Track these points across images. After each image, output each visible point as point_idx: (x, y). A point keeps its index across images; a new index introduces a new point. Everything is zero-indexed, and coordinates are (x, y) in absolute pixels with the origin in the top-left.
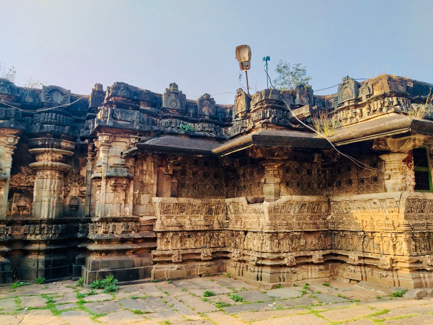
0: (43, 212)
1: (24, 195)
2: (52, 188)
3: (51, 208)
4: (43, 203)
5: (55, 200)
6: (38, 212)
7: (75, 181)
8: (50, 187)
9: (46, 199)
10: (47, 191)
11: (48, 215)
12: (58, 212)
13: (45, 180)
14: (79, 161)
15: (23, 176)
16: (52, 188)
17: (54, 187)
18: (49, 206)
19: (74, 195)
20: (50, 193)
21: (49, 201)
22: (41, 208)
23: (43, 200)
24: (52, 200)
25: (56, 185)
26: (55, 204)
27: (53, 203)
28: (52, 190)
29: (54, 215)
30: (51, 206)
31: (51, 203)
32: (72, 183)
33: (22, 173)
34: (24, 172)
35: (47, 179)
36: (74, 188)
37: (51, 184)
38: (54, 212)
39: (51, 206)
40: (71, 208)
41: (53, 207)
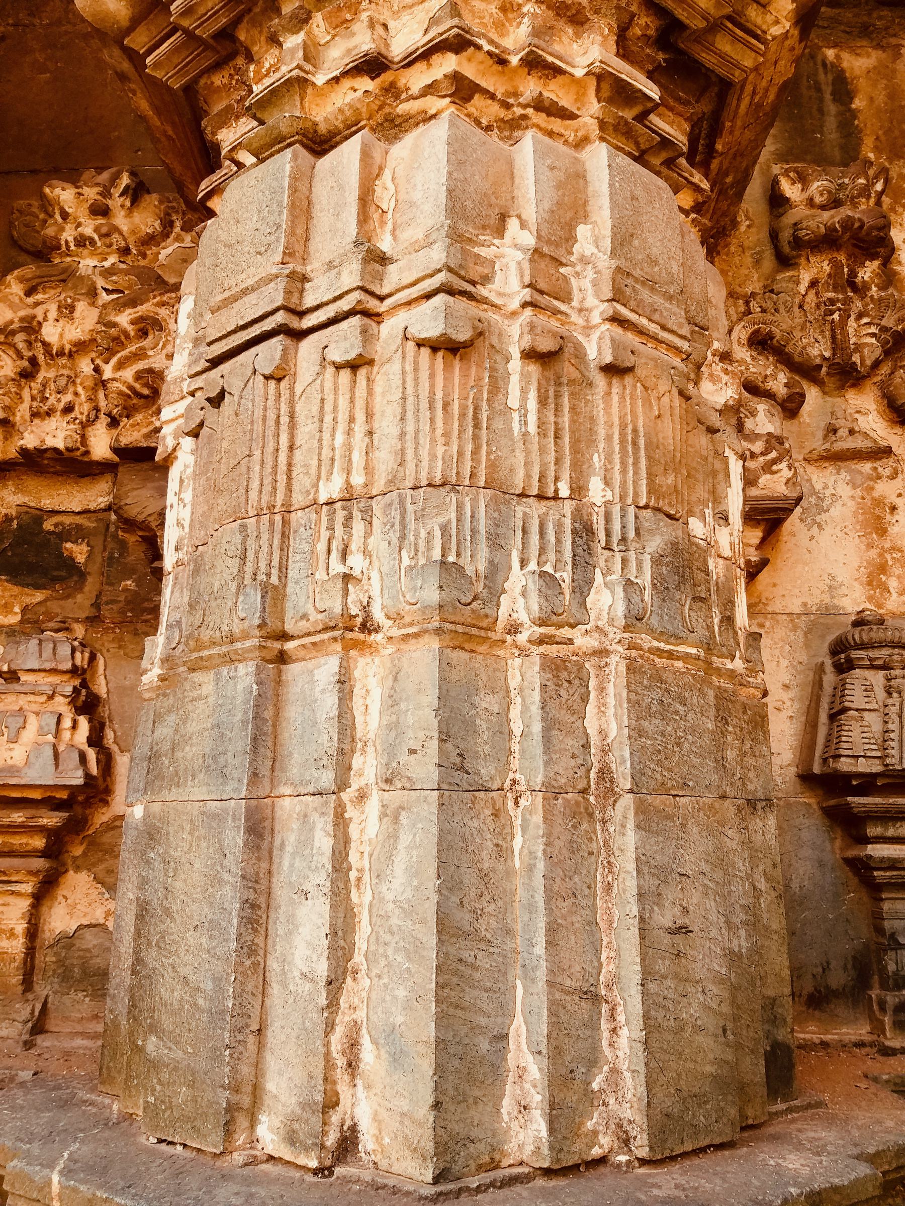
0: (301, 943)
1: (81, 603)
2: (509, 284)
3: (527, 836)
4: (313, 678)
5: (606, 601)
6: (192, 962)
7: (845, 374)
8: (462, 284)
9: (389, 574)
10: (388, 378)
11: (463, 1070)
12: (707, 960)
13: (347, 155)
14: (843, 89)
15: (67, 311)
16: (509, 284)
17: (547, 292)
18: (463, 776)
19: (853, 600)
20: (479, 418)
21: (466, 624)
22: (259, 830)
23: (309, 600)
24: (519, 601)
25: (592, 241)
26: (607, 717)
27: (566, 679)
28: (515, 335)
29: (623, 1046)
30: (528, 766)
31: (523, 675)
32: (791, 407)
33: (67, 277)
34: (87, 263)
35: (392, 127)
36: (836, 487)
37: (476, 214)
38: (621, 961)
39: (528, 766)
40: (849, 825)
41: (577, 803)
